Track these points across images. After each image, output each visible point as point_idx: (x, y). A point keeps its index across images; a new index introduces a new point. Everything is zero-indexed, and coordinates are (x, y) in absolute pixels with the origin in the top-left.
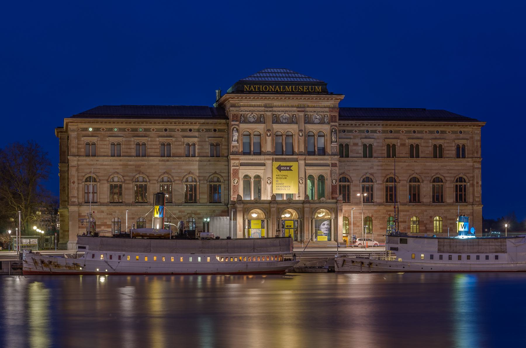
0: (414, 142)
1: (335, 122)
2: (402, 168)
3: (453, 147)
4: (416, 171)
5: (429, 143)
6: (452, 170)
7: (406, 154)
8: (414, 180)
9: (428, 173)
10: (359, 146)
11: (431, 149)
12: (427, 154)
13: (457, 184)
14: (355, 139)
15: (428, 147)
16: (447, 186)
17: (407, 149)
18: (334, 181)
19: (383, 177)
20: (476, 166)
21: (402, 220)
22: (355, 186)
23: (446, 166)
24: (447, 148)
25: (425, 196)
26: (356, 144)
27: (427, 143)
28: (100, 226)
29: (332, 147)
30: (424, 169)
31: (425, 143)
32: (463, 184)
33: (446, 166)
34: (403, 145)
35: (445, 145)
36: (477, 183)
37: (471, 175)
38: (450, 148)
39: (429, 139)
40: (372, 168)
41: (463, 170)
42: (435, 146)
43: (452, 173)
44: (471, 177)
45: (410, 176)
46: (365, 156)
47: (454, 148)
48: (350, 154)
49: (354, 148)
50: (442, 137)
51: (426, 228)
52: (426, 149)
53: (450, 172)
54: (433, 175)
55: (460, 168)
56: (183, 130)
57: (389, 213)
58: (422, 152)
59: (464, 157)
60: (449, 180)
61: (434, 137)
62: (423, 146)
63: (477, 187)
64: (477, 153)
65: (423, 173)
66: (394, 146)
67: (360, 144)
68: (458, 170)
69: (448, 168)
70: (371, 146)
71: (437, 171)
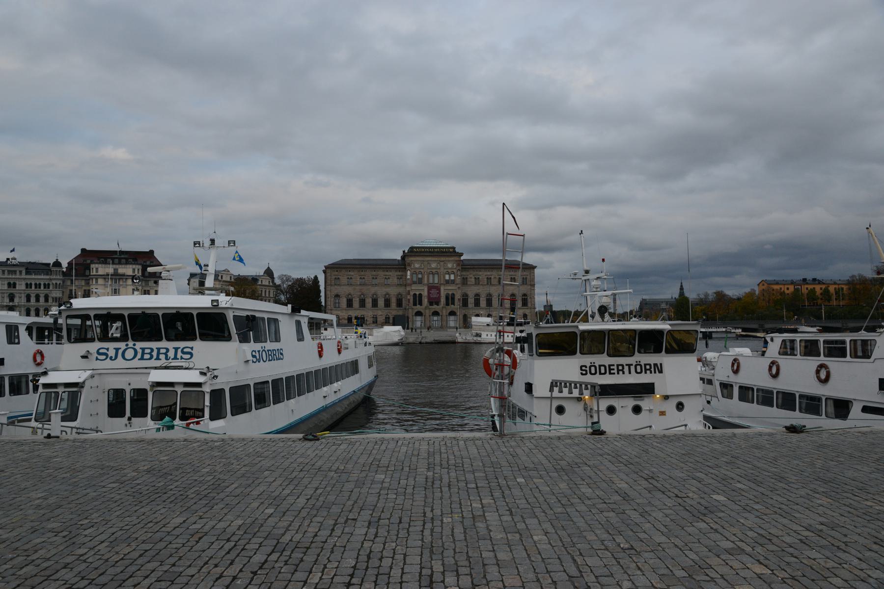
17: (497, 280)
26: (471, 278)
28: (341, 319)
29: (459, 280)
34: (495, 278)
40: (478, 290)
46: (476, 284)
48: (468, 283)
56: (383, 271)
59: (526, 284)
66: (490, 278)
70: (478, 278)
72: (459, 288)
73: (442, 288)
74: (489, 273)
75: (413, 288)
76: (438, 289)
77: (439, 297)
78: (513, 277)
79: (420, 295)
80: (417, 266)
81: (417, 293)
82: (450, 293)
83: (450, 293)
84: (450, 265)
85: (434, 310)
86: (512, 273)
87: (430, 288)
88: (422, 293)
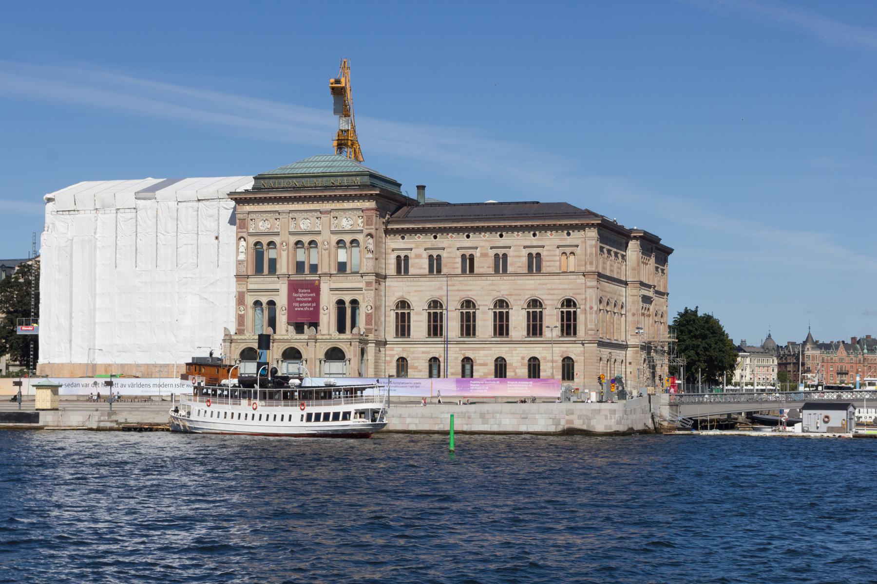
0: (500, 252)
1: (372, 225)
2: (482, 288)
3: (556, 256)
4: (502, 293)
5: (522, 251)
6: (555, 289)
7: (488, 267)
8: (501, 303)
9: (520, 295)
10: (423, 258)
11: (525, 260)
12: (518, 267)
13: (562, 310)
14: (418, 248)
15: (520, 257)
16: (547, 313)
17: (491, 261)
18: (369, 308)
19: (456, 301)
20: (589, 284)
21: (482, 362)
22: (418, 314)
23: (546, 284)
24: (548, 258)
25: (514, 328)
26: (419, 256)
27: (519, 251)
30: (514, 289)
31: (516, 251)
32: (572, 310)
33: (546, 284)
35: (544, 253)
36: (591, 308)
37: (583, 297)
38: (551, 258)
39: (519, 246)
40: (440, 288)
41: (570, 289)
42: (530, 255)
43: (554, 294)
44: (582, 300)
45: (494, 299)
47: (558, 258)
48: (412, 271)
49: (417, 261)
50: (540, 243)
51: (516, 374)
52: (517, 261)
53: (552, 292)
54: (527, 297)
55: (566, 286)
57: (463, 352)
58: (512, 264)
60: (549, 305)
61: (528, 243)
62: (513, 256)
63: (591, 313)
64: (591, 263)
65: (512, 295)
67: (425, 255)
68: (564, 289)
69: (549, 286)
71: (532, 292)
72: (368, 284)
73: (325, 287)
74: (467, 243)
75: (251, 287)
76: (315, 289)
77: (316, 312)
78: (534, 251)
79: (272, 303)
80: (263, 226)
81: (264, 300)
82: (347, 299)
83: (347, 299)
84: (345, 223)
85: (287, 346)
86: (534, 241)
87: (294, 287)
88: (276, 299)
